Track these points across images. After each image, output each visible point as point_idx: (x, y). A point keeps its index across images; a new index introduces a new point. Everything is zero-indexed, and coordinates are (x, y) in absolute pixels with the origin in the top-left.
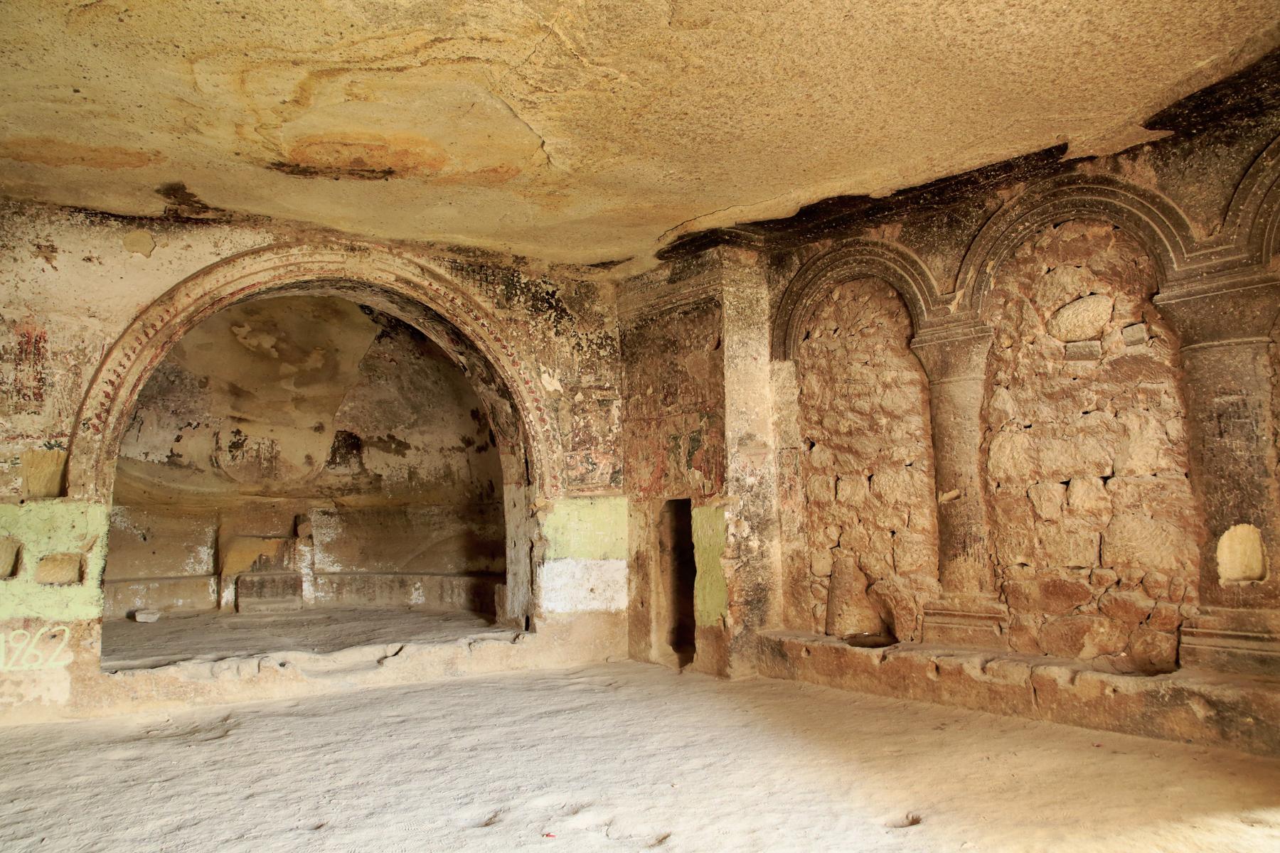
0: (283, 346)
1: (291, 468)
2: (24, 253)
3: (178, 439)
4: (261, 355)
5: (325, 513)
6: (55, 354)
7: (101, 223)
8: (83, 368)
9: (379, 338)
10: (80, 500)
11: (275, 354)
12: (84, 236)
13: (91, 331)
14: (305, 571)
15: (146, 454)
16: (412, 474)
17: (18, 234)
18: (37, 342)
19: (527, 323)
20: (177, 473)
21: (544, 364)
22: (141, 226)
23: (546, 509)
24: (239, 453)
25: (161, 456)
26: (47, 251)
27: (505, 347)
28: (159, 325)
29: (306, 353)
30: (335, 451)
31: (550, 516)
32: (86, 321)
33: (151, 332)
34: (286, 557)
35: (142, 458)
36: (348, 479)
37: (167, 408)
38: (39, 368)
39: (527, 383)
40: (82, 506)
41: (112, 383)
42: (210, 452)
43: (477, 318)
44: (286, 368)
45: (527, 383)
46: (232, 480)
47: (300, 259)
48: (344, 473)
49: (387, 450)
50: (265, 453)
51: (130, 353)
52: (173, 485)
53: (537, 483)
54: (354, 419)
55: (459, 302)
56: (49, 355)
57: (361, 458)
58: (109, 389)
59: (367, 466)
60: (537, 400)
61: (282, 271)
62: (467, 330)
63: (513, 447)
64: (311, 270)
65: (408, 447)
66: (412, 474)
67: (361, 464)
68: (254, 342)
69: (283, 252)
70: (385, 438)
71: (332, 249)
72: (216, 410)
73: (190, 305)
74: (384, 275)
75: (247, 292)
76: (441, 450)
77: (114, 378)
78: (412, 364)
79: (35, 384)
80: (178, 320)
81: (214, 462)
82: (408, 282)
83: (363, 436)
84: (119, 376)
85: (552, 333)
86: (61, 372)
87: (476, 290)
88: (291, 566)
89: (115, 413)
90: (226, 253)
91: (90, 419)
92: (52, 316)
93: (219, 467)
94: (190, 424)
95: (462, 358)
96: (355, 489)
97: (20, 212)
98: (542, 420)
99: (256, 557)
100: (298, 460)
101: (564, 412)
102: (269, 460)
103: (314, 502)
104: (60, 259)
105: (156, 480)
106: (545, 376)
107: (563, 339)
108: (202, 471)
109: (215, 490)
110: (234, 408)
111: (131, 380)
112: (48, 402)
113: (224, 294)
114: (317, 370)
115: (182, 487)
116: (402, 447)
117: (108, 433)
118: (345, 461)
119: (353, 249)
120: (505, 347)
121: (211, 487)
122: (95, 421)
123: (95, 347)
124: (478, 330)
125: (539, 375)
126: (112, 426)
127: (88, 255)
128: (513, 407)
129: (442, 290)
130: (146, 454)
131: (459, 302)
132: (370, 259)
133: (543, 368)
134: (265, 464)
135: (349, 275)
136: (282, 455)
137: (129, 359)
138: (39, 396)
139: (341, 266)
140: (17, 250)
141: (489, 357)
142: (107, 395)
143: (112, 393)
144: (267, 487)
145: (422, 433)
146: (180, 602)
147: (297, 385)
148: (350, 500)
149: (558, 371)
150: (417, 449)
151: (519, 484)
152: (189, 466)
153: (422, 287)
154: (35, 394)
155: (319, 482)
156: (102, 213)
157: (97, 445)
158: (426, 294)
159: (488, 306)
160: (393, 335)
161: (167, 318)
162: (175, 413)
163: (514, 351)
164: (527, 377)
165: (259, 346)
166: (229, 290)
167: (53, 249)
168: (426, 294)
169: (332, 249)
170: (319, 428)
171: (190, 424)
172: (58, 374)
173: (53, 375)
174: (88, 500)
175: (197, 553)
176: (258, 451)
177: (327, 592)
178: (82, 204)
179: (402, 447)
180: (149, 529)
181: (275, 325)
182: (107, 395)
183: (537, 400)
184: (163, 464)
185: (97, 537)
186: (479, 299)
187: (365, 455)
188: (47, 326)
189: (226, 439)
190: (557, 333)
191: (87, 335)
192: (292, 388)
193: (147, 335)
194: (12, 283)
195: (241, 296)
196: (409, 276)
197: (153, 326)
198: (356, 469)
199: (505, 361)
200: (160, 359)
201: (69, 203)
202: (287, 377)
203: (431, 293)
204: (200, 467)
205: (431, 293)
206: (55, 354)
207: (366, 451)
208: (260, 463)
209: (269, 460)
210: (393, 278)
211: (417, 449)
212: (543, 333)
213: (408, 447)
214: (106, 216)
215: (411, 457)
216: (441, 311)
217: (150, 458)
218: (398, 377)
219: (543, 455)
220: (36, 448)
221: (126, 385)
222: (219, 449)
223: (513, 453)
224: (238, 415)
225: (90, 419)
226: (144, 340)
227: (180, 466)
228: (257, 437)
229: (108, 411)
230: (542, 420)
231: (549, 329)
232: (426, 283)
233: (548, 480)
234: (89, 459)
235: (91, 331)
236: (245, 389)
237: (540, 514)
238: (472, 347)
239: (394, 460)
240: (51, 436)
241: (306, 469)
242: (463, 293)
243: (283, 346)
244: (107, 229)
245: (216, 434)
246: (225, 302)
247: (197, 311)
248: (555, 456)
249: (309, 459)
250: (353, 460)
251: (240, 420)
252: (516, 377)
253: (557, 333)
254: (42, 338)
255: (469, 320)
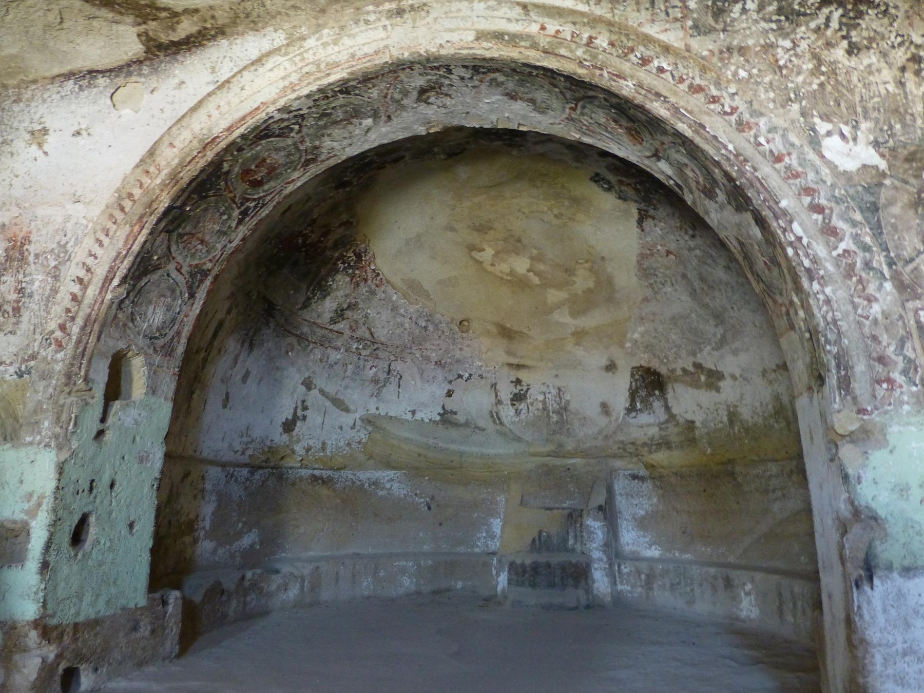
0: (541, 267)
1: (584, 421)
2: (19, 145)
3: (449, 394)
4: (518, 283)
5: (635, 477)
6: (37, 256)
7: (89, 85)
8: (62, 268)
9: (640, 222)
10: (31, 443)
11: (536, 280)
12: (73, 107)
13: (73, 221)
14: (596, 554)
15: (413, 412)
16: (733, 416)
17: (16, 124)
18: (23, 244)
19: (769, 47)
20: (454, 433)
21: (825, 117)
22: (130, 74)
23: (866, 437)
24: (522, 406)
25: (431, 413)
26: (39, 135)
27: (715, 100)
28: (137, 192)
29: (570, 271)
30: (633, 395)
31: (878, 457)
32: (72, 209)
33: (127, 204)
34: (571, 535)
35: (409, 416)
36: (654, 431)
37: (428, 359)
38: (21, 277)
39: (779, 159)
40: (32, 450)
41: (80, 280)
42: (490, 408)
43: (645, 61)
44: (554, 296)
45: (779, 159)
46: (519, 439)
47: (321, 54)
48: (647, 424)
49: (696, 385)
50: (552, 405)
51: (102, 237)
52: (453, 447)
53: (832, 380)
54: (648, 347)
55: (602, 42)
56: (31, 258)
57: (666, 400)
58: (76, 289)
59: (675, 411)
60: (808, 191)
61: (294, 78)
62: (627, 88)
63: (788, 313)
64: (337, 64)
65: (720, 376)
66: (733, 416)
67: (667, 408)
68: (504, 267)
69: (294, 50)
70: (691, 369)
71: (367, 22)
72: (485, 353)
73: (175, 157)
74: (455, 37)
75: (251, 122)
76: (764, 373)
77: (82, 273)
78: (690, 249)
79: (14, 296)
80: (158, 181)
81: (496, 418)
82: (498, 36)
83: (663, 370)
84: (88, 270)
85: (839, 53)
86: (40, 277)
87: (645, 15)
88: (578, 547)
89: (80, 321)
90: (224, 75)
91: (53, 332)
92: (41, 211)
93: (501, 423)
94: (460, 376)
95: (663, 165)
96: (665, 444)
97: (17, 101)
98: (830, 232)
99: (536, 534)
100: (593, 411)
101: (896, 210)
102: (558, 412)
103: (618, 463)
104: (52, 141)
105: (431, 441)
106: (833, 147)
107: (871, 58)
108: (483, 430)
109: (501, 451)
110: (509, 353)
111: (101, 272)
112: (25, 316)
113: (216, 132)
114: (589, 291)
115: (463, 448)
116: (714, 378)
117: (71, 346)
118: (647, 406)
119: (400, 12)
120: (715, 100)
121: (499, 449)
122: (59, 334)
123: (77, 239)
124: (650, 80)
125: (815, 142)
126: (74, 338)
127: (76, 128)
128: (760, 221)
129: (567, 31)
130: (413, 412)
131: (602, 42)
132: (430, 19)
133: (823, 127)
134: (555, 418)
135: (396, 53)
136: (573, 406)
137: (101, 244)
138: (17, 310)
139: (381, 45)
140: (14, 144)
141: (682, 127)
142: (74, 298)
143: (79, 294)
144: (561, 445)
145: (735, 353)
146: (460, 585)
147: (574, 314)
148: (659, 457)
149: (865, 125)
150: (734, 377)
151: (810, 388)
152: (467, 424)
153: (529, 37)
154: (14, 309)
155: (620, 437)
156: (90, 72)
157: (58, 367)
158: (534, 46)
159: (674, 37)
160: (652, 212)
161: (146, 181)
162: (438, 363)
163: (738, 102)
164: (778, 146)
165: (512, 273)
166: (225, 124)
167: (45, 131)
168: (534, 46)
169: (367, 22)
170: (611, 367)
171: (460, 376)
172: (38, 281)
173: (32, 282)
174: (39, 444)
175: (489, 525)
176: (544, 402)
177: (634, 586)
178: (66, 69)
179: (714, 378)
180: (433, 498)
181: (519, 241)
182: (74, 298)
183: (808, 191)
184: (434, 422)
185: (42, 497)
186: (652, 30)
187: (670, 395)
188: (33, 224)
189: (506, 391)
190: (853, 50)
191: (69, 226)
192: (568, 320)
193: (122, 209)
194: (8, 180)
195: (241, 130)
196: (501, 25)
197: (130, 196)
198: (662, 416)
199: (717, 126)
200: (141, 239)
201: (56, 71)
202: (558, 306)
203: (543, 42)
204: (481, 424)
205: (543, 42)
206: (37, 256)
207: (670, 391)
208: (548, 416)
209: (558, 412)
210: (471, 36)
211: (734, 377)
212: (816, 57)
213: (720, 376)
214: (93, 73)
215: (728, 391)
216: (569, 67)
217: (418, 416)
218: (684, 276)
219: (842, 310)
220: (7, 377)
221: (95, 280)
222: (499, 402)
223: (792, 327)
224: (515, 361)
225: (53, 332)
226: (119, 216)
227: (456, 425)
228: (539, 384)
229: (73, 319)
230: (830, 232)
231: (829, 45)
232: (534, 28)
233: (860, 367)
234: (47, 386)
235: (73, 221)
236: (516, 328)
237: (847, 452)
238: (655, 125)
239: (706, 397)
240: (24, 361)
241: (602, 421)
242: (610, 24)
243: (541, 267)
244: (95, 90)
245: (494, 386)
246: (223, 145)
247: (182, 165)
248: (876, 309)
249: (605, 408)
250: (657, 404)
251: (519, 367)
252: (749, 151)
253: (853, 50)
254: (27, 240)
255: (626, 67)
